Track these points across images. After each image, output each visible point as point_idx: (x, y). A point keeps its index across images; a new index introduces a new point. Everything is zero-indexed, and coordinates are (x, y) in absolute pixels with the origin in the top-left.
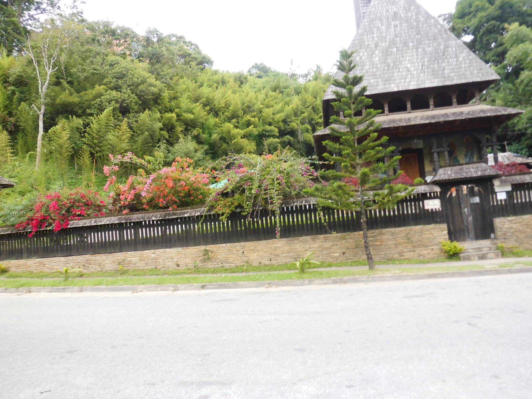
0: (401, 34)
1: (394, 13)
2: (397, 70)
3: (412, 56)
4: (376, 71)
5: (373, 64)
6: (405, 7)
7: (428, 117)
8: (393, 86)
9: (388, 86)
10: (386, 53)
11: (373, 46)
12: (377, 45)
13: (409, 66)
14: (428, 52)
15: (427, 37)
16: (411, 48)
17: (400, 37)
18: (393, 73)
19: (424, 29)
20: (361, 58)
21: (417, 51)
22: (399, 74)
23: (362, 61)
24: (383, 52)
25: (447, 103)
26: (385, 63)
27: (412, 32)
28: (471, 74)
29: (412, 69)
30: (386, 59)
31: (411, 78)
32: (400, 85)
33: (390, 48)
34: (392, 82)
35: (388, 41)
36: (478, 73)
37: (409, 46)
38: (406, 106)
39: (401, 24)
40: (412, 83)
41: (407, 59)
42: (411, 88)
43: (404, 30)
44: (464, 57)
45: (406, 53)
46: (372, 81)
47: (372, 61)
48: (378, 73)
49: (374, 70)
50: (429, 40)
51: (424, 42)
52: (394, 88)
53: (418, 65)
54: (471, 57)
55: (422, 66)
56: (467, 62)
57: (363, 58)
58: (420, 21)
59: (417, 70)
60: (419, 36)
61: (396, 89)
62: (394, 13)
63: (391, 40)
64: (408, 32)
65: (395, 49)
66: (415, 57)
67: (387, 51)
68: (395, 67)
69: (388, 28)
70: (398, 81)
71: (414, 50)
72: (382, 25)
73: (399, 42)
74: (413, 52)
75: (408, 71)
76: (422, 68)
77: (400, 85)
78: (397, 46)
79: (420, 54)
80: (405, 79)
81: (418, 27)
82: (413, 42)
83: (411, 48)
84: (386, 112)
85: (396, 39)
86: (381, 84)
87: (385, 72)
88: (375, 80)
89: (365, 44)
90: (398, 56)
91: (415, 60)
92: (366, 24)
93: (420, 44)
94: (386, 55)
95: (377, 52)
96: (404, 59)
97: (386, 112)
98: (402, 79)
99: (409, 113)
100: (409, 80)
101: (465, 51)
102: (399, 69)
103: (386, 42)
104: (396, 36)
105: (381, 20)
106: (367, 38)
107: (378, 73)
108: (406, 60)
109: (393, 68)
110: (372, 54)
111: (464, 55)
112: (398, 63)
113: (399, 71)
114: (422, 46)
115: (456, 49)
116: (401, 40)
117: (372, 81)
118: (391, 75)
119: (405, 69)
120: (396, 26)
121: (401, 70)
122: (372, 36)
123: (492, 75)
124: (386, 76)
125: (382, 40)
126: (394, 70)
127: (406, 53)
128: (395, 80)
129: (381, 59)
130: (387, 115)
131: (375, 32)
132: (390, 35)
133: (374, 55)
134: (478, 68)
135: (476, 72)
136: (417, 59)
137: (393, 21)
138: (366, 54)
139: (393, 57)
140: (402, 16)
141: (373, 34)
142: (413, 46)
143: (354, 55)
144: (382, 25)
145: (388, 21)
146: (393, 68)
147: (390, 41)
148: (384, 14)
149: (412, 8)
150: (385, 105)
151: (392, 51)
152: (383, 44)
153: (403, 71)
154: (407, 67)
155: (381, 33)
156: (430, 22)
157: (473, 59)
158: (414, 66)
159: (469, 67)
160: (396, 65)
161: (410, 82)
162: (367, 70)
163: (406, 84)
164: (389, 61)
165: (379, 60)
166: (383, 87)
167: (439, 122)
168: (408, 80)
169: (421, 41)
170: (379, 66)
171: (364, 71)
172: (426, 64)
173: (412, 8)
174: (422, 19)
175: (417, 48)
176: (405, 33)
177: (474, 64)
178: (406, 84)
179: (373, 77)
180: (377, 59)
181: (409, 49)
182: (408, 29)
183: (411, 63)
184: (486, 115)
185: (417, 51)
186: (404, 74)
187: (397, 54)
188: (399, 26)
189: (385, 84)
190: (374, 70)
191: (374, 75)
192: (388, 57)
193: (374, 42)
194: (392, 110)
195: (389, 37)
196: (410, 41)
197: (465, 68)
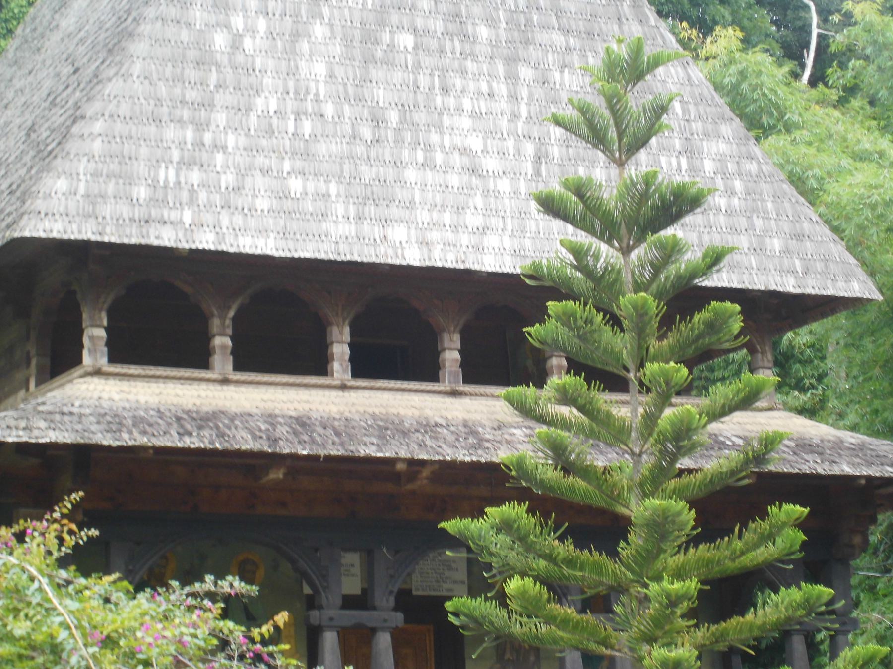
2: (420, 156)
3: (491, 95)
5: (300, 95)
7: (185, 419)
8: (398, 233)
9: (377, 232)
13: (475, 143)
14: (564, 96)
15: (559, 13)
16: (482, 49)
18: (397, 164)
20: (236, 44)
21: (512, 78)
22: (429, 175)
23: (240, 58)
24: (347, 41)
25: (299, 356)
26: (360, 99)
29: (491, 164)
30: (366, 80)
31: (487, 211)
32: (434, 235)
34: (395, 211)
36: (787, 251)
37: (474, 40)
40: (491, 240)
41: (467, 104)
42: (489, 263)
44: (721, 159)
45: (463, 72)
46: (295, 185)
47: (292, 73)
48: (322, 148)
49: (307, 127)
50: (566, 32)
51: (542, 37)
52: (405, 245)
53: (518, 152)
54: (752, 167)
55: (538, 159)
56: (738, 185)
57: (248, 43)
59: (514, 175)
61: (414, 257)
66: (503, 105)
67: (370, 39)
68: (408, 136)
70: (423, 216)
71: (501, 69)
75: (473, 171)
76: (538, 173)
77: (434, 235)
78: (419, 23)
79: (524, 92)
80: (460, 209)
82: (492, 22)
83: (482, 49)
84: (340, 368)
86: (341, 211)
88: (311, 186)
90: (423, 81)
91: (504, 124)
93: (527, 42)
94: (368, 60)
95: (319, 30)
96: (451, 101)
97: (340, 368)
99: (454, 394)
101: (726, 130)
102: (428, 148)
107: (322, 148)
108: (460, 110)
109: (399, 142)
110: (296, 36)
111: (723, 147)
112: (420, 117)
113: (428, 164)
114: (534, 53)
115: (685, 111)
117: (295, 185)
119: (457, 159)
121: (439, 157)
124: (367, 173)
126: (406, 154)
127: (463, 72)
128: (411, 205)
129: (340, 72)
130: (343, 387)
133: (304, 46)
134: (786, 227)
135: (776, 244)
136: (515, 116)
139: (398, 76)
142: (494, 44)
143: (660, 70)
146: (399, 142)
150: (216, 323)
151: (392, 46)
153: (447, 168)
154: (464, 151)
157: (760, 175)
158: (502, 153)
159: (750, 212)
161: (484, 230)
162: (265, 115)
163: (465, 239)
164: (381, 95)
165: (331, 76)
166: (349, 229)
167: (479, 462)
169: (529, 23)
170: (329, 110)
171: (253, 120)
172: (555, 151)
175: (511, 61)
177: (770, 205)
178: (465, 239)
179: (299, 164)
180: (320, 69)
181: (474, 57)
183: (489, 134)
184: (836, 470)
185: (512, 78)
187: (418, 66)
189: (359, 218)
190: (307, 127)
191: (307, 155)
192: (376, 73)
194: (370, 365)
197: (730, 213)
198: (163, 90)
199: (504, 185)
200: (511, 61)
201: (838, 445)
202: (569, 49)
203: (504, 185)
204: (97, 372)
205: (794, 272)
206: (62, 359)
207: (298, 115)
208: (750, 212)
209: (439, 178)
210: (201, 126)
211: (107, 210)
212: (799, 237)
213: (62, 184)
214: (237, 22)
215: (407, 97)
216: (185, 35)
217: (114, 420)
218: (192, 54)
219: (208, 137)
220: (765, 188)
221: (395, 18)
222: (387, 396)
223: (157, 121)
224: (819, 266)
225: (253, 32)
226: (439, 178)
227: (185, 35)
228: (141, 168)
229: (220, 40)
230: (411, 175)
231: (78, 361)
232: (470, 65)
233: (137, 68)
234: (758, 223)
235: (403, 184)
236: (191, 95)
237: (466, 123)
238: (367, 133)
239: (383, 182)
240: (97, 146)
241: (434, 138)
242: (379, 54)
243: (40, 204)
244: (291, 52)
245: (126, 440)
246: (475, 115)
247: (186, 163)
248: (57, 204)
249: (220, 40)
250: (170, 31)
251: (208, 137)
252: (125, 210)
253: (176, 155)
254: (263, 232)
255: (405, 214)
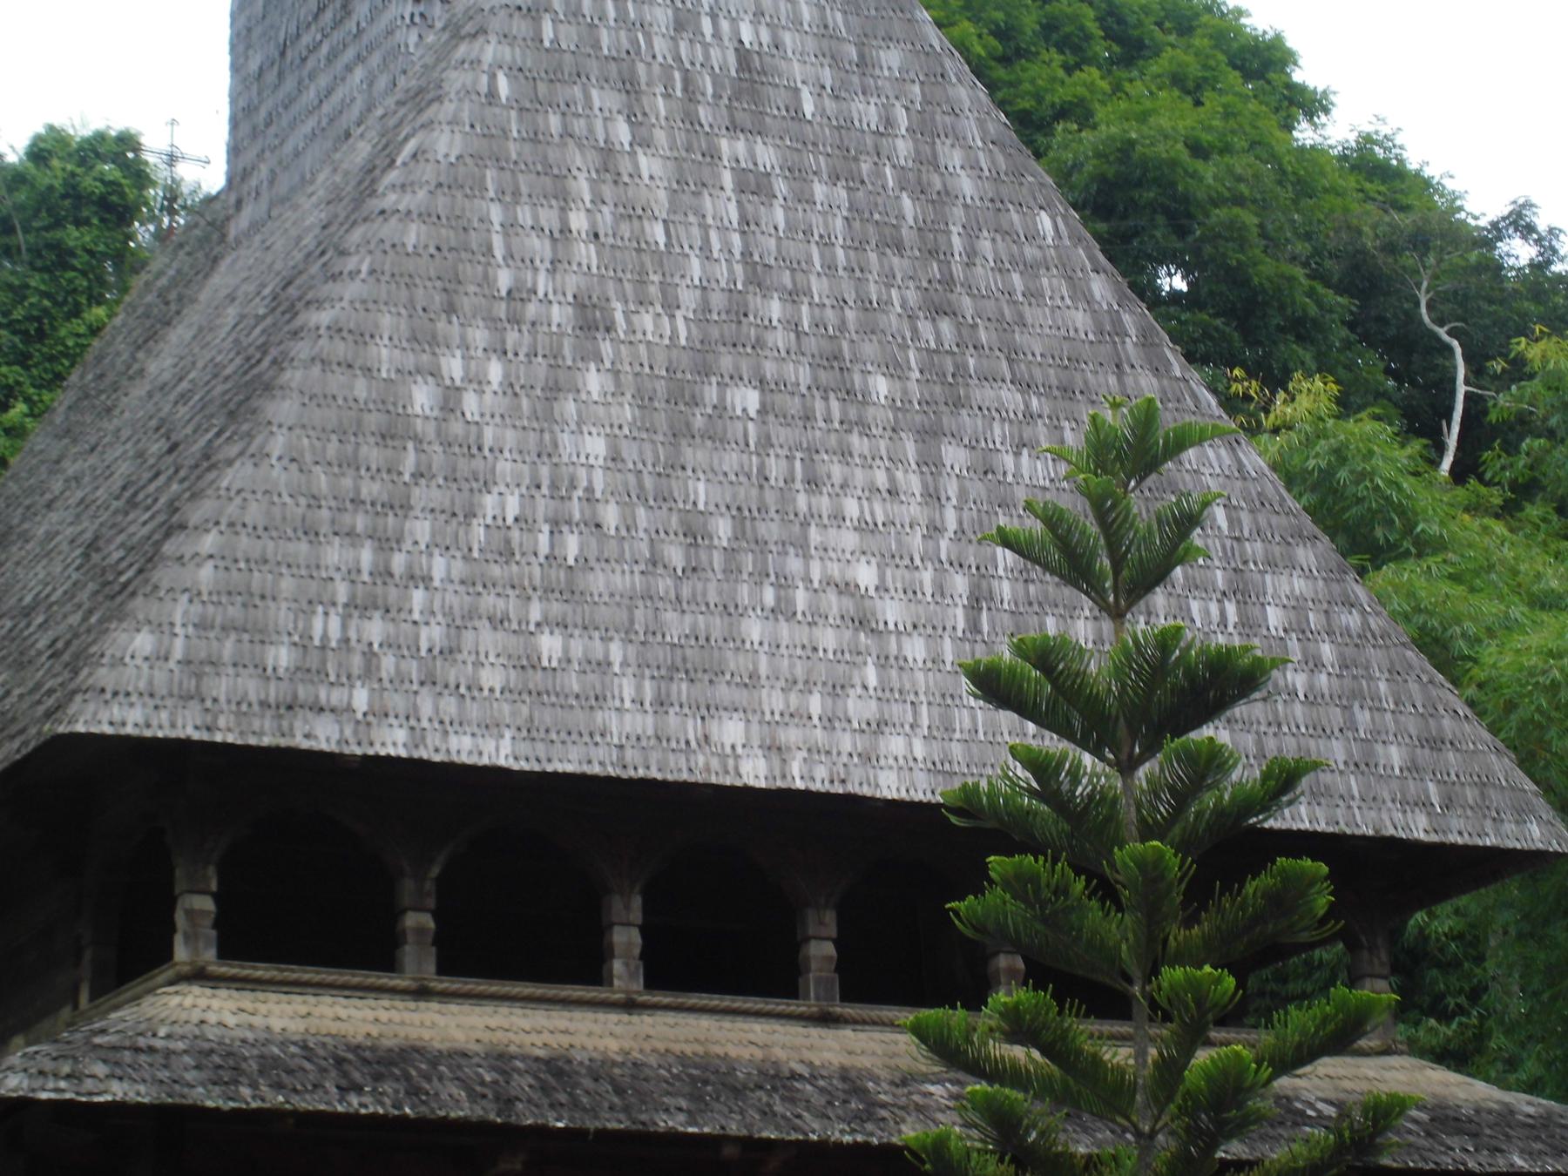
0: (799, 267)
1: (743, 54)
3: (893, 492)
4: (584, 561)
5: (561, 489)
6: (825, 31)
8: (731, 731)
9: (692, 729)
10: (675, 405)
11: (560, 314)
12: (591, 319)
13: (866, 575)
14: (1021, 494)
15: (1013, 354)
16: (879, 415)
17: (793, 296)
18: (731, 610)
19: (983, 275)
21: (930, 464)
22: (784, 630)
23: (456, 428)
24: (644, 401)
26: (664, 498)
27: (888, 279)
28: (1363, 765)
29: (892, 611)
31: (885, 692)
33: (705, 371)
34: (723, 692)
35: (689, 299)
36: (1413, 768)
37: (866, 401)
38: (396, 914)
39: (797, 174)
40: (895, 744)
41: (851, 508)
42: (889, 786)
43: (826, 243)
44: (1296, 606)
45: (845, 453)
46: (550, 645)
47: (548, 452)
48: (597, 582)
49: (572, 545)
51: (983, 394)
52: (740, 752)
53: (940, 590)
54: (1352, 620)
55: (977, 601)
56: (1327, 651)
57: (471, 403)
58: (947, 195)
60: (945, 326)
61: (754, 772)
62: (743, 54)
63: (718, 300)
64: (857, 271)
65: (748, 399)
66: (913, 509)
67: (683, 397)
68: (748, 562)
69: (691, 179)
70: (774, 700)
71: (910, 448)
72: (642, 141)
73: (780, 338)
74: (895, 460)
75: (862, 622)
76: (974, 627)
77: (791, 735)
78: (770, 369)
79: (952, 488)
80: (837, 689)
81: (935, 252)
82: (895, 370)
83: (879, 415)
84: (624, 973)
85: (755, 301)
86: (628, 692)
87: (664, 584)
89: (487, 281)
90: (776, 469)
91: (916, 542)
92: (503, 86)
93: (958, 404)
94: (680, 433)
95: (594, 382)
96: (824, 503)
97: (624, 973)
98: (808, 686)
100: (871, 710)
101: (1305, 555)
102: (784, 584)
103: (671, 306)
104: (758, 276)
105: (630, 87)
106: (510, 227)
107: (597, 582)
108: (838, 517)
109: (732, 571)
110: (554, 390)
111: (1300, 585)
112: (770, 530)
113: (782, 611)
115: (1233, 522)
116: (795, 326)
117: (550, 645)
118: (718, 625)
119: (833, 603)
120: (753, 185)
121: (801, 598)
122: (548, 217)
123: (1522, 813)
124: (676, 625)
125: (642, 282)
127: (845, 453)
128: (752, 681)
129: (630, 452)
131: (582, 187)
132: (706, 248)
133: (569, 408)
135: (1395, 756)
136: (935, 530)
137: (734, 128)
138: (495, 371)
139: (731, 460)
140: (808, 108)
141: (564, 199)
142: (898, 406)
143: (1191, 454)
144: (642, 141)
145: (692, 120)
146: (732, 571)
147: (705, 307)
148: (660, 45)
149: (891, 58)
150: (408, 886)
151: (721, 408)
152: (646, 321)
153: (816, 617)
154: (847, 588)
155: (632, 213)
156: (1033, 236)
157: (1366, 633)
159: (1349, 699)
160: (761, 544)
161: (879, 726)
162: (498, 525)
164: (701, 491)
165: (615, 457)
166: (644, 723)
167: (867, 1145)
168: (859, 708)
169: (960, 370)
170: (611, 516)
171: (479, 533)
172: (1005, 590)
173: (891, 58)
174: (966, 185)
175: (930, 435)
176: (830, 267)
178: (846, 742)
179: (556, 608)
180: (596, 446)
181: (864, 428)
182: (857, 245)
183: (887, 559)
185: (930, 464)
186: (828, 639)
187: (766, 442)
188: (781, 186)
189: (661, 703)
191: (571, 593)
192: (692, 455)
193: (572, 282)
194: (680, 969)
195: (695, 267)
196: (869, 349)
198: (322, 481)
199: (916, 649)
200: (930, 435)
201: (1506, 1116)
202: (1029, 416)
203: (916, 649)
204: (199, 976)
205: (1426, 805)
206: (137, 956)
207: (557, 524)
208: (1349, 699)
209: (802, 634)
210: (386, 543)
211: (220, 687)
212: (1435, 743)
213: (143, 642)
214: (454, 367)
215: (747, 494)
216: (361, 388)
217: (223, 1060)
218: (373, 420)
219: (398, 562)
220: (1374, 656)
221: (726, 362)
222: (705, 1023)
223: (311, 533)
224: (1471, 794)
225: (478, 381)
226: (802, 634)
227: (361, 388)
228: (282, 615)
229: (422, 397)
230: (754, 629)
231: (166, 955)
232: (856, 441)
233: (278, 445)
234: (1363, 717)
235: (740, 644)
236: (371, 489)
237: (849, 539)
238: (675, 555)
239: (703, 641)
240: (206, 575)
241: (794, 564)
242: (699, 422)
243: (104, 676)
244: (546, 418)
245: (247, 1097)
246: (865, 527)
247: (360, 607)
248: (134, 676)
249: (422, 397)
250: (337, 381)
251: (398, 562)
252: (251, 687)
253: (342, 591)
254: (492, 727)
255: (741, 696)
